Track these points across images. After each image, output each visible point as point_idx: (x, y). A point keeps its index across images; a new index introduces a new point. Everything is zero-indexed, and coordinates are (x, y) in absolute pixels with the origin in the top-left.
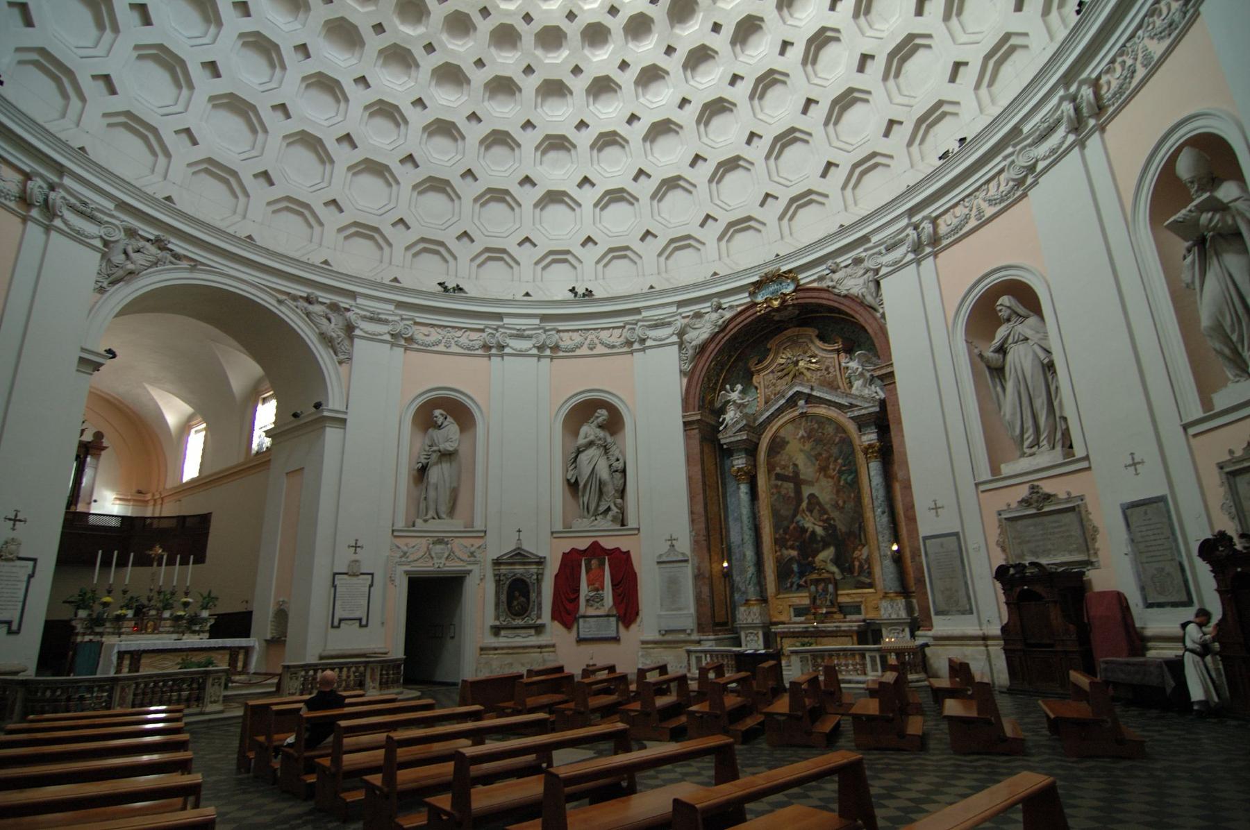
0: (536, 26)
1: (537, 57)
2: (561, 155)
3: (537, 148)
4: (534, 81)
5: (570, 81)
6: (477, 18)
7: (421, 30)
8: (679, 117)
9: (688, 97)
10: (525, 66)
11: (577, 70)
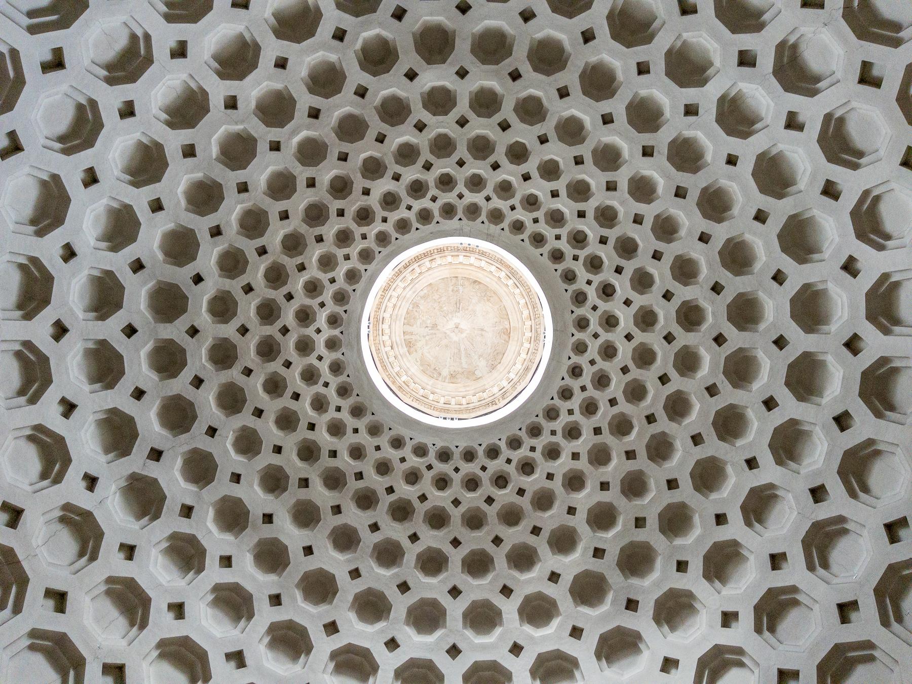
0: (262, 147)
1: (236, 123)
2: (110, 54)
3: (147, 37)
4: (216, 101)
5: (184, 136)
6: (317, 101)
7: (359, 45)
8: (56, 240)
9: (72, 262)
10: (239, 104)
11: (189, 152)
